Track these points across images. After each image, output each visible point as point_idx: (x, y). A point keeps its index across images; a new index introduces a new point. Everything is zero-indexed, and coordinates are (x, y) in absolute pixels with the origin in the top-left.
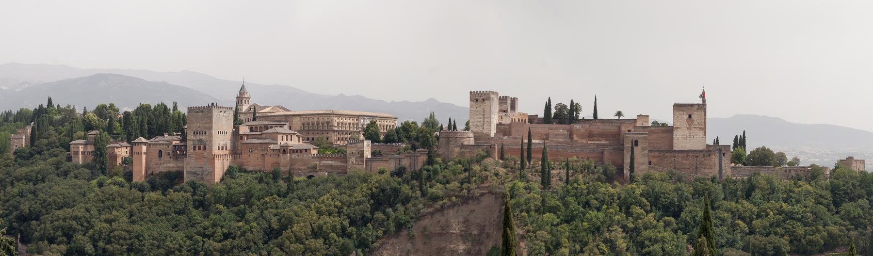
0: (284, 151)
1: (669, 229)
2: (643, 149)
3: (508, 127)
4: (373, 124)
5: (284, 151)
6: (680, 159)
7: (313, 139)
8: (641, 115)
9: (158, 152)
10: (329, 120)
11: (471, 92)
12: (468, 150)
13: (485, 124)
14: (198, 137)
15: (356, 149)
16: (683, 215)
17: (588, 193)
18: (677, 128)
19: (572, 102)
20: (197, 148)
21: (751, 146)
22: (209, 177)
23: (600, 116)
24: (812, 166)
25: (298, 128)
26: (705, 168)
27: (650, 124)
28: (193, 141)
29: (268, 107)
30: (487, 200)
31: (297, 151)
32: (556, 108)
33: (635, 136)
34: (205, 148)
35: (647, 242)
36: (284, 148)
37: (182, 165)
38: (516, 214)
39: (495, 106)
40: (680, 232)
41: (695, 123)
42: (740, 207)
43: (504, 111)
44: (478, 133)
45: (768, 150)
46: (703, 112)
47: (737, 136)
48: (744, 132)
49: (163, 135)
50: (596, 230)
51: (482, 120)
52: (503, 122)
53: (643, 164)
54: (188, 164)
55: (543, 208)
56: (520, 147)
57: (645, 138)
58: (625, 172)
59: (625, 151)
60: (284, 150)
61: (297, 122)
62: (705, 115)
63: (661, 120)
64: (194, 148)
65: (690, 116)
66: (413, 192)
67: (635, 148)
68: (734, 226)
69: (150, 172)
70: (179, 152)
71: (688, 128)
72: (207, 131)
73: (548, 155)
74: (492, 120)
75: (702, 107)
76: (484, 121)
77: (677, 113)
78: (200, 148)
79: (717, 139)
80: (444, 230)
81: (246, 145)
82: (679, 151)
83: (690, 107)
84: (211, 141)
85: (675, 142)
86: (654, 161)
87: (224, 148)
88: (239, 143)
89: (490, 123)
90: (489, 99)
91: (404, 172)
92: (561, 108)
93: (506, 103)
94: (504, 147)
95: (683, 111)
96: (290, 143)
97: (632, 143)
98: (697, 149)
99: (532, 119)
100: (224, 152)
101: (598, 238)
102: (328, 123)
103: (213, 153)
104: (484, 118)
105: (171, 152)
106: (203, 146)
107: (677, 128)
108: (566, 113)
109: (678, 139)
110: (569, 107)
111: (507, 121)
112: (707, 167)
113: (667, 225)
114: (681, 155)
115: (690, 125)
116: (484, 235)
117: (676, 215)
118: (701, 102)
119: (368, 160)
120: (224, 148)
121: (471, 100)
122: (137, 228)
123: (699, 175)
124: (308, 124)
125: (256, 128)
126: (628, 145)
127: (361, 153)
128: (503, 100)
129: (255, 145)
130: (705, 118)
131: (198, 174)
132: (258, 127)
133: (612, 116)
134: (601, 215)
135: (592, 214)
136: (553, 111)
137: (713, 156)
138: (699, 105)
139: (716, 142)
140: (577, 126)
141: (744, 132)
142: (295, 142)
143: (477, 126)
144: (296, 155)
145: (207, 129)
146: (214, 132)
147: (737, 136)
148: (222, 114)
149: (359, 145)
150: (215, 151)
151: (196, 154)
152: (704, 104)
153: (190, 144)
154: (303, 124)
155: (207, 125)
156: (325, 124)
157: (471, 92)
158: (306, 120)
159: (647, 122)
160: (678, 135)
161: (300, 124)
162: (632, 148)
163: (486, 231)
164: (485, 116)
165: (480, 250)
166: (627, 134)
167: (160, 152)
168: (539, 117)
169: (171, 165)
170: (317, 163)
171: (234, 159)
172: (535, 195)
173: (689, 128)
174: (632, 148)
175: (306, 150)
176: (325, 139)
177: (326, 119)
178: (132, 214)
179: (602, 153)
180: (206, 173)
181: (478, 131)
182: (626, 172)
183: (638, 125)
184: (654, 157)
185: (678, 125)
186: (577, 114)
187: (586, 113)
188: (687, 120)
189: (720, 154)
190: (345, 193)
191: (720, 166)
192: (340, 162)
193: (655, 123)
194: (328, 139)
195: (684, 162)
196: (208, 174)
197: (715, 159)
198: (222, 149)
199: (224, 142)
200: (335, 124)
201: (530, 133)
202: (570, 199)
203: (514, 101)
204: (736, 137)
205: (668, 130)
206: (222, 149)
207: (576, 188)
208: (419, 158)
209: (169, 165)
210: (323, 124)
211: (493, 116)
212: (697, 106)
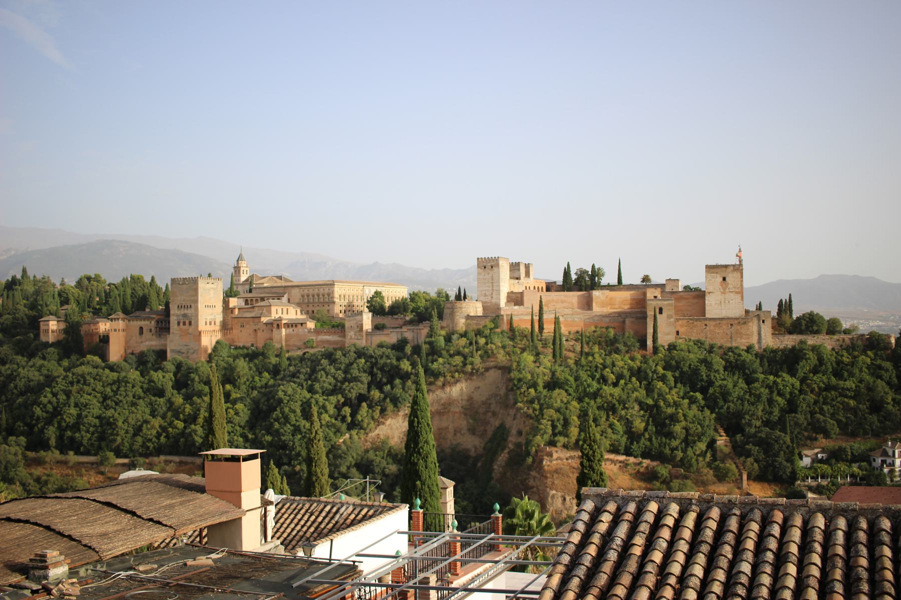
0: (278, 325)
1: (694, 407)
2: (669, 317)
3: (519, 296)
4: (378, 294)
5: (278, 325)
6: (712, 328)
7: (313, 312)
8: (670, 279)
9: (138, 329)
10: (331, 291)
11: (478, 259)
12: (475, 322)
13: (494, 293)
14: (183, 312)
15: (355, 322)
16: (711, 391)
17: (605, 367)
18: (709, 293)
19: (593, 266)
20: (181, 324)
21: (798, 311)
22: (195, 356)
23: (625, 281)
24: (871, 334)
25: (297, 301)
26: (741, 338)
27: (680, 289)
28: (177, 316)
29: (265, 277)
30: (493, 375)
31: (292, 326)
32: (576, 274)
33: (659, 302)
34: (190, 323)
35: (667, 422)
36: (278, 322)
37: (164, 342)
38: (523, 390)
39: (504, 271)
40: (707, 412)
41: (731, 286)
42: (779, 380)
43: (517, 279)
44: (486, 302)
45: (817, 314)
46: (739, 274)
47: (781, 300)
48: (790, 295)
49: (144, 310)
50: (611, 409)
51: (490, 288)
52: (515, 291)
53: (668, 334)
54: (172, 341)
55: (553, 384)
56: (529, 317)
57: (669, 305)
58: (648, 343)
59: (648, 319)
60: (276, 324)
61: (296, 293)
62: (742, 277)
63: (692, 284)
64: (179, 324)
65: (724, 279)
66: (412, 369)
67: (658, 316)
68: (770, 402)
69: (129, 351)
70: (163, 327)
71: (722, 293)
72: (193, 305)
73: (562, 326)
74: (501, 288)
75: (738, 268)
76: (493, 290)
77: (709, 276)
78: (184, 324)
79: (760, 304)
80: (445, 408)
81: (236, 320)
82: (711, 319)
83: (724, 269)
84: (197, 316)
85: (707, 308)
86: (681, 330)
87: (213, 323)
88: (229, 318)
89: (498, 291)
90: (498, 265)
91: (182, 366)
92: (582, 274)
93: (519, 270)
94: (514, 318)
95: (717, 273)
96: (285, 316)
97: (655, 311)
98: (733, 316)
99: (550, 287)
100: (212, 327)
101: (611, 417)
102: (329, 295)
103: (200, 329)
104: (493, 286)
105: (153, 329)
106: (190, 321)
107: (709, 293)
108: (587, 279)
109: (711, 305)
110: (590, 273)
111: (518, 289)
112: (744, 337)
113: (693, 401)
114: (713, 323)
115: (724, 289)
116: (490, 414)
117: (704, 391)
118: (738, 263)
119: (368, 334)
120: (213, 323)
121: (478, 267)
122: (110, 413)
123: (734, 344)
124: (308, 296)
125: (252, 300)
126: (650, 313)
127: (360, 327)
128: (514, 267)
129: (247, 319)
130: (742, 281)
131: (183, 353)
132: (254, 299)
133: (638, 281)
134: (617, 391)
135: (607, 390)
136: (574, 277)
137: (751, 324)
138: (734, 266)
139: (759, 308)
140: (596, 293)
141: (790, 295)
142: (293, 314)
143: (485, 295)
144: (291, 330)
145: (192, 303)
146: (201, 306)
147: (781, 300)
148: (210, 286)
149: (358, 317)
150: (202, 326)
151: (181, 330)
152: (741, 265)
153: (173, 320)
154: (303, 296)
155: (193, 298)
156: (326, 296)
157: (478, 259)
158: (306, 291)
159: (678, 287)
160: (709, 301)
161: (299, 296)
162: (655, 316)
163: (492, 409)
164: (494, 283)
165: (486, 430)
166: (653, 300)
167: (141, 328)
168: (558, 284)
169: (153, 343)
170: (314, 338)
171: (224, 335)
172: (545, 370)
173: (724, 293)
174: (655, 316)
175: (302, 324)
176: (326, 312)
177: (327, 291)
178: (105, 398)
179: (624, 322)
180: (192, 351)
181: (487, 300)
182: (650, 343)
183: (667, 290)
184: (682, 326)
185: (711, 289)
186: (598, 279)
187: (609, 278)
188: (721, 282)
189: (759, 320)
190: (340, 369)
191: (759, 334)
192: (339, 336)
193: (687, 288)
194: (328, 311)
195: (717, 331)
196: (194, 353)
197: (753, 326)
198: (210, 324)
199: (212, 317)
200: (336, 295)
201: (541, 302)
202: (584, 375)
203: (527, 267)
204: (781, 301)
205: (698, 295)
206: (210, 324)
207: (591, 362)
208: (423, 331)
209: (150, 343)
210: (323, 295)
211: (501, 284)
212: (732, 268)
